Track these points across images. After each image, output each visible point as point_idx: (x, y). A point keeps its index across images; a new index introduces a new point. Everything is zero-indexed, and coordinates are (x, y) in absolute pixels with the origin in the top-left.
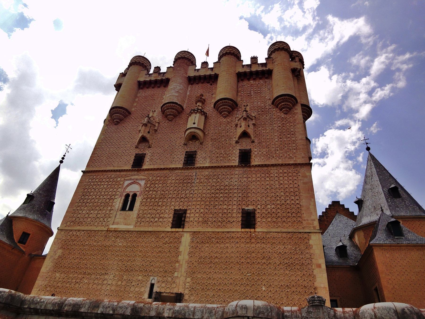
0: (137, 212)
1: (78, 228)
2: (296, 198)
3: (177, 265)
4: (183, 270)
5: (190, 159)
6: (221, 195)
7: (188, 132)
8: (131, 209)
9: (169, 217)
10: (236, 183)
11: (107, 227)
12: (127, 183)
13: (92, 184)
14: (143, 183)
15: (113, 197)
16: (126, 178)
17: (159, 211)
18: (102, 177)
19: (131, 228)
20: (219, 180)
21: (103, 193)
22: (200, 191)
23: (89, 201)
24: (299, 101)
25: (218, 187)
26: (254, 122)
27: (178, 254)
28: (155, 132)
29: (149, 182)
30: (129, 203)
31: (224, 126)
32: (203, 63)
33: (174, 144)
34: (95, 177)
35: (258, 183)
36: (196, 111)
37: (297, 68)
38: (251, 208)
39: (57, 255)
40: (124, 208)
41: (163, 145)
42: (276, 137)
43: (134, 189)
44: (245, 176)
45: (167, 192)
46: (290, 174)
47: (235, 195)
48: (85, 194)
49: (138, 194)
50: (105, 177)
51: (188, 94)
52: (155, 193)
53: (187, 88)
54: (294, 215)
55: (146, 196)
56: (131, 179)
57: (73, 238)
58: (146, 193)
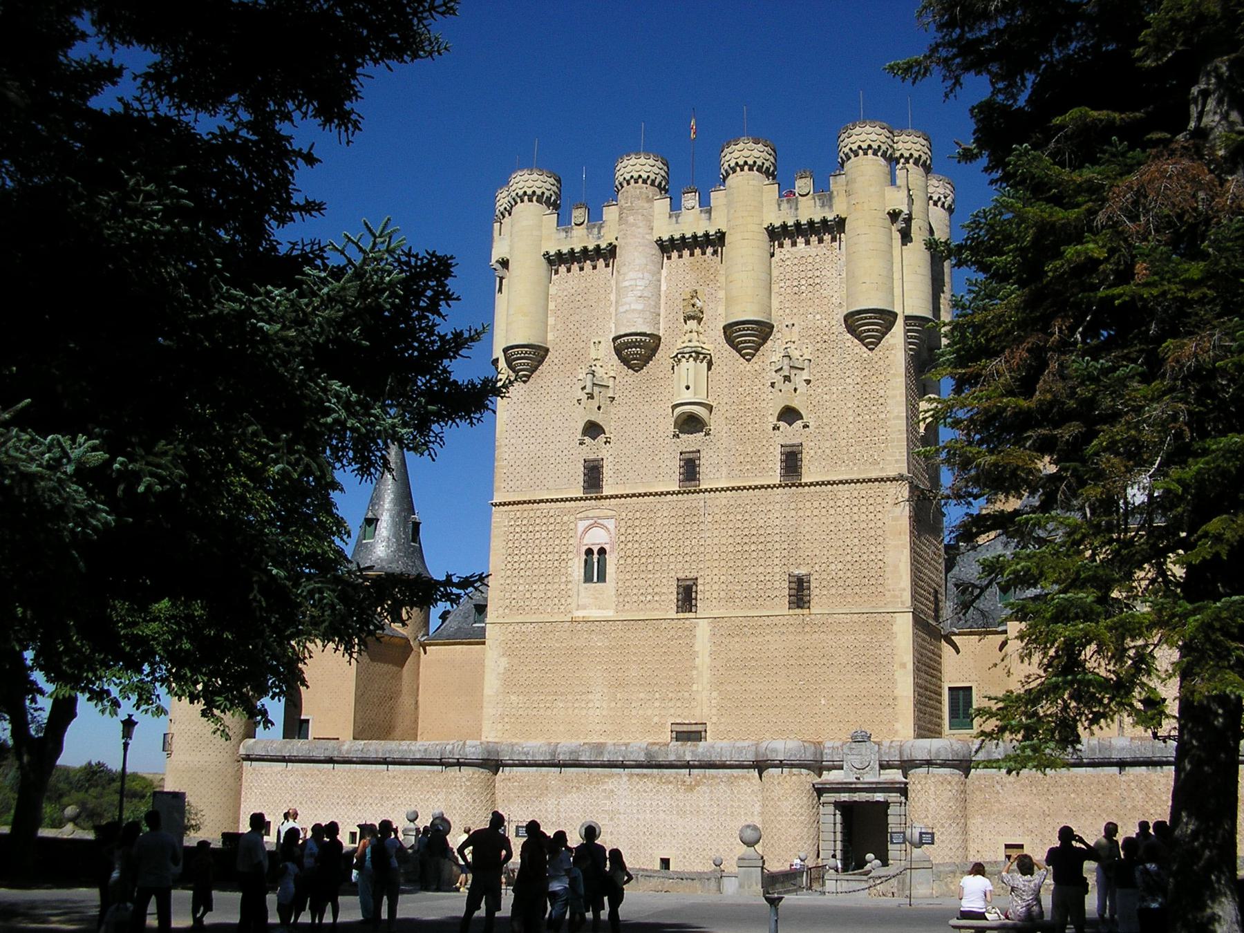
0: (614, 584)
1: (520, 619)
2: (880, 548)
3: (695, 672)
4: (705, 681)
5: (690, 469)
6: (753, 547)
8: (602, 578)
9: (671, 595)
10: (777, 522)
11: (570, 615)
12: (582, 525)
13: (518, 529)
14: (611, 524)
15: (564, 556)
18: (532, 514)
19: (609, 614)
20: (747, 516)
21: (544, 550)
22: (716, 541)
23: (522, 566)
24: (898, 310)
25: (746, 532)
26: (805, 375)
27: (694, 655)
30: (595, 565)
31: (749, 382)
33: (653, 433)
35: (816, 520)
37: (901, 212)
38: (802, 571)
40: (588, 578)
42: (851, 412)
43: (597, 538)
44: (793, 506)
45: (658, 544)
46: (871, 501)
47: (777, 546)
48: (510, 551)
49: (607, 547)
51: (663, 288)
52: (636, 545)
53: (659, 273)
54: (873, 581)
55: (622, 554)
56: (587, 518)
57: (518, 637)
58: (622, 546)
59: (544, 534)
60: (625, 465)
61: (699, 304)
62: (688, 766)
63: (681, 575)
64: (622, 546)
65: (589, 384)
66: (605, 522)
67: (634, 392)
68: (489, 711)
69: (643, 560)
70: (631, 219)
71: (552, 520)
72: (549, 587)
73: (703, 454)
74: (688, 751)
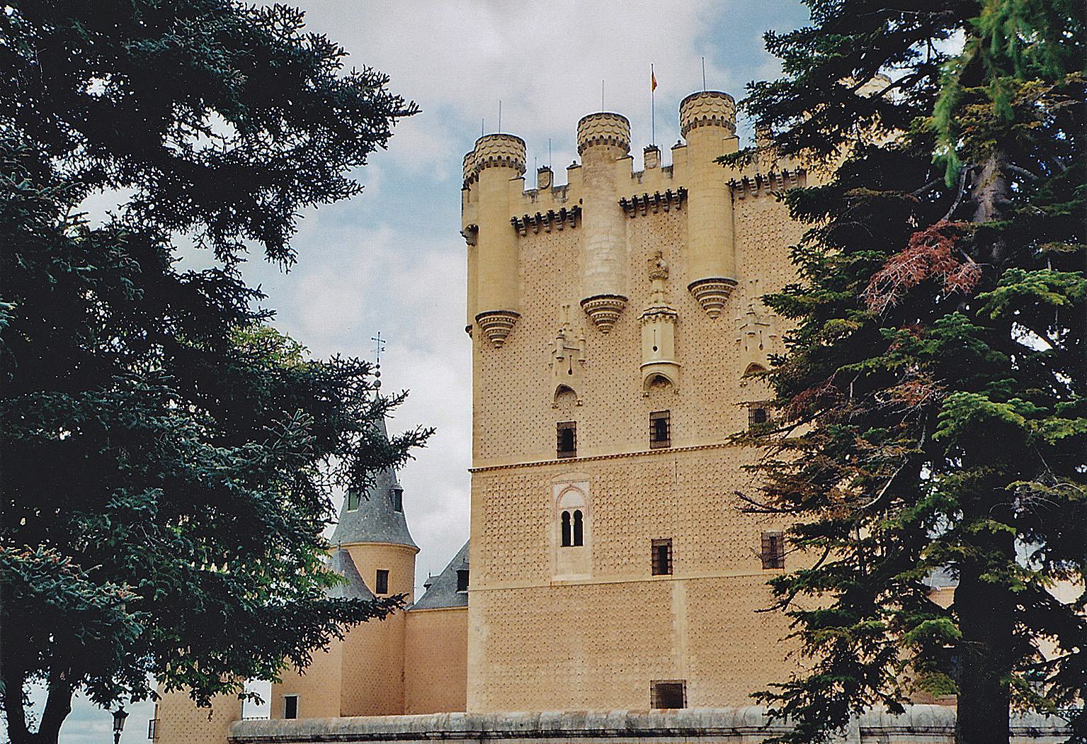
0: (590, 547)
1: (501, 585)
5: (660, 430)
7: (647, 372)
8: (579, 542)
11: (548, 581)
12: (557, 489)
13: (496, 495)
14: (585, 487)
16: (553, 480)
17: (626, 544)
19: (587, 578)
27: (670, 618)
28: (582, 365)
29: (597, 486)
30: (572, 530)
32: (646, 151)
33: (624, 395)
34: (496, 480)
36: (654, 316)
39: (484, 636)
40: (566, 543)
41: (603, 398)
43: (572, 502)
45: (632, 506)
50: (515, 478)
52: (611, 508)
55: (597, 517)
56: (562, 482)
58: (597, 508)
59: (522, 499)
60: (597, 428)
61: (663, 264)
62: (668, 733)
63: (656, 537)
64: (597, 508)
65: (559, 349)
66: (580, 485)
67: (603, 355)
68: (474, 681)
69: (618, 522)
70: (594, 181)
71: (529, 485)
72: (528, 552)
73: (673, 414)
74: (670, 718)
